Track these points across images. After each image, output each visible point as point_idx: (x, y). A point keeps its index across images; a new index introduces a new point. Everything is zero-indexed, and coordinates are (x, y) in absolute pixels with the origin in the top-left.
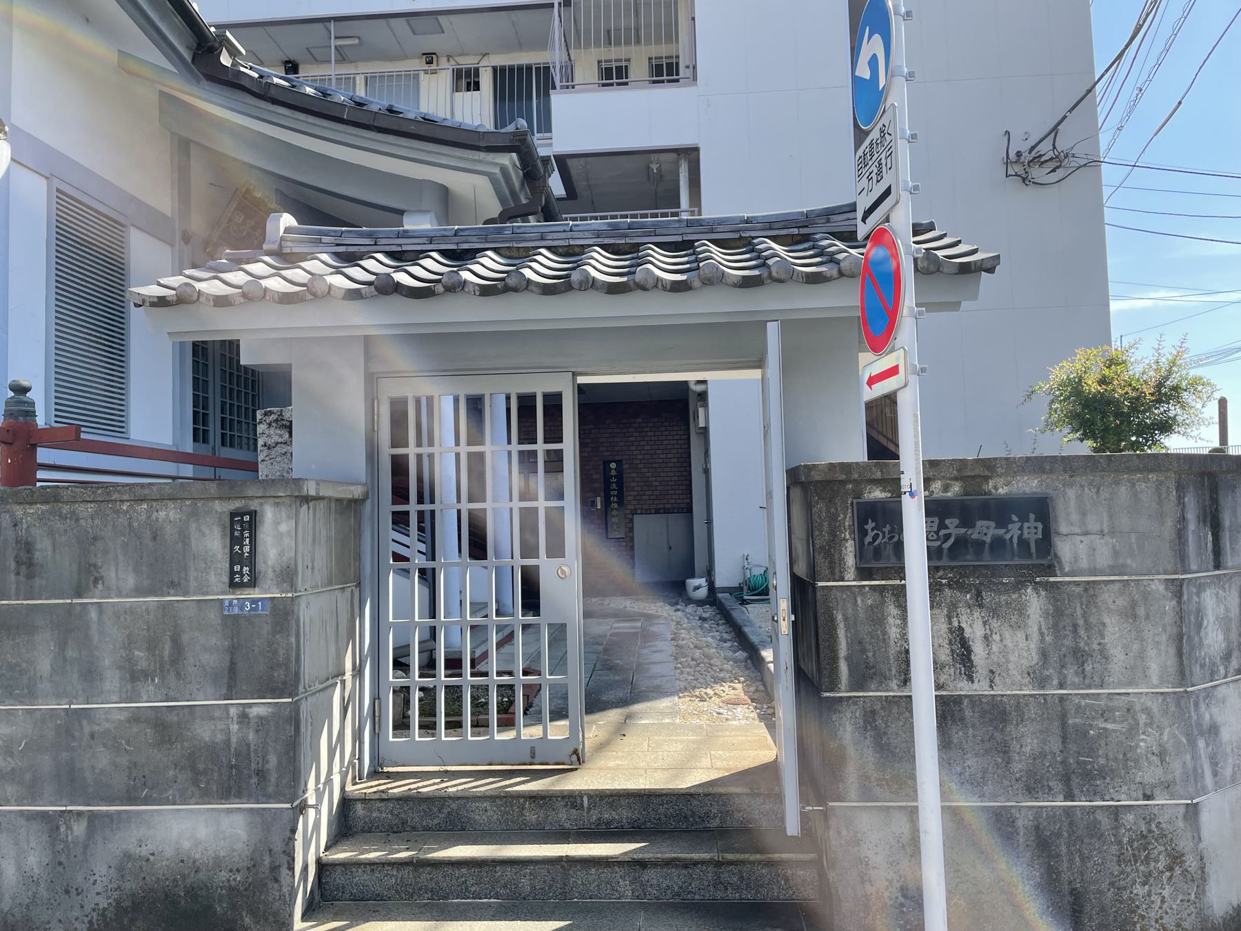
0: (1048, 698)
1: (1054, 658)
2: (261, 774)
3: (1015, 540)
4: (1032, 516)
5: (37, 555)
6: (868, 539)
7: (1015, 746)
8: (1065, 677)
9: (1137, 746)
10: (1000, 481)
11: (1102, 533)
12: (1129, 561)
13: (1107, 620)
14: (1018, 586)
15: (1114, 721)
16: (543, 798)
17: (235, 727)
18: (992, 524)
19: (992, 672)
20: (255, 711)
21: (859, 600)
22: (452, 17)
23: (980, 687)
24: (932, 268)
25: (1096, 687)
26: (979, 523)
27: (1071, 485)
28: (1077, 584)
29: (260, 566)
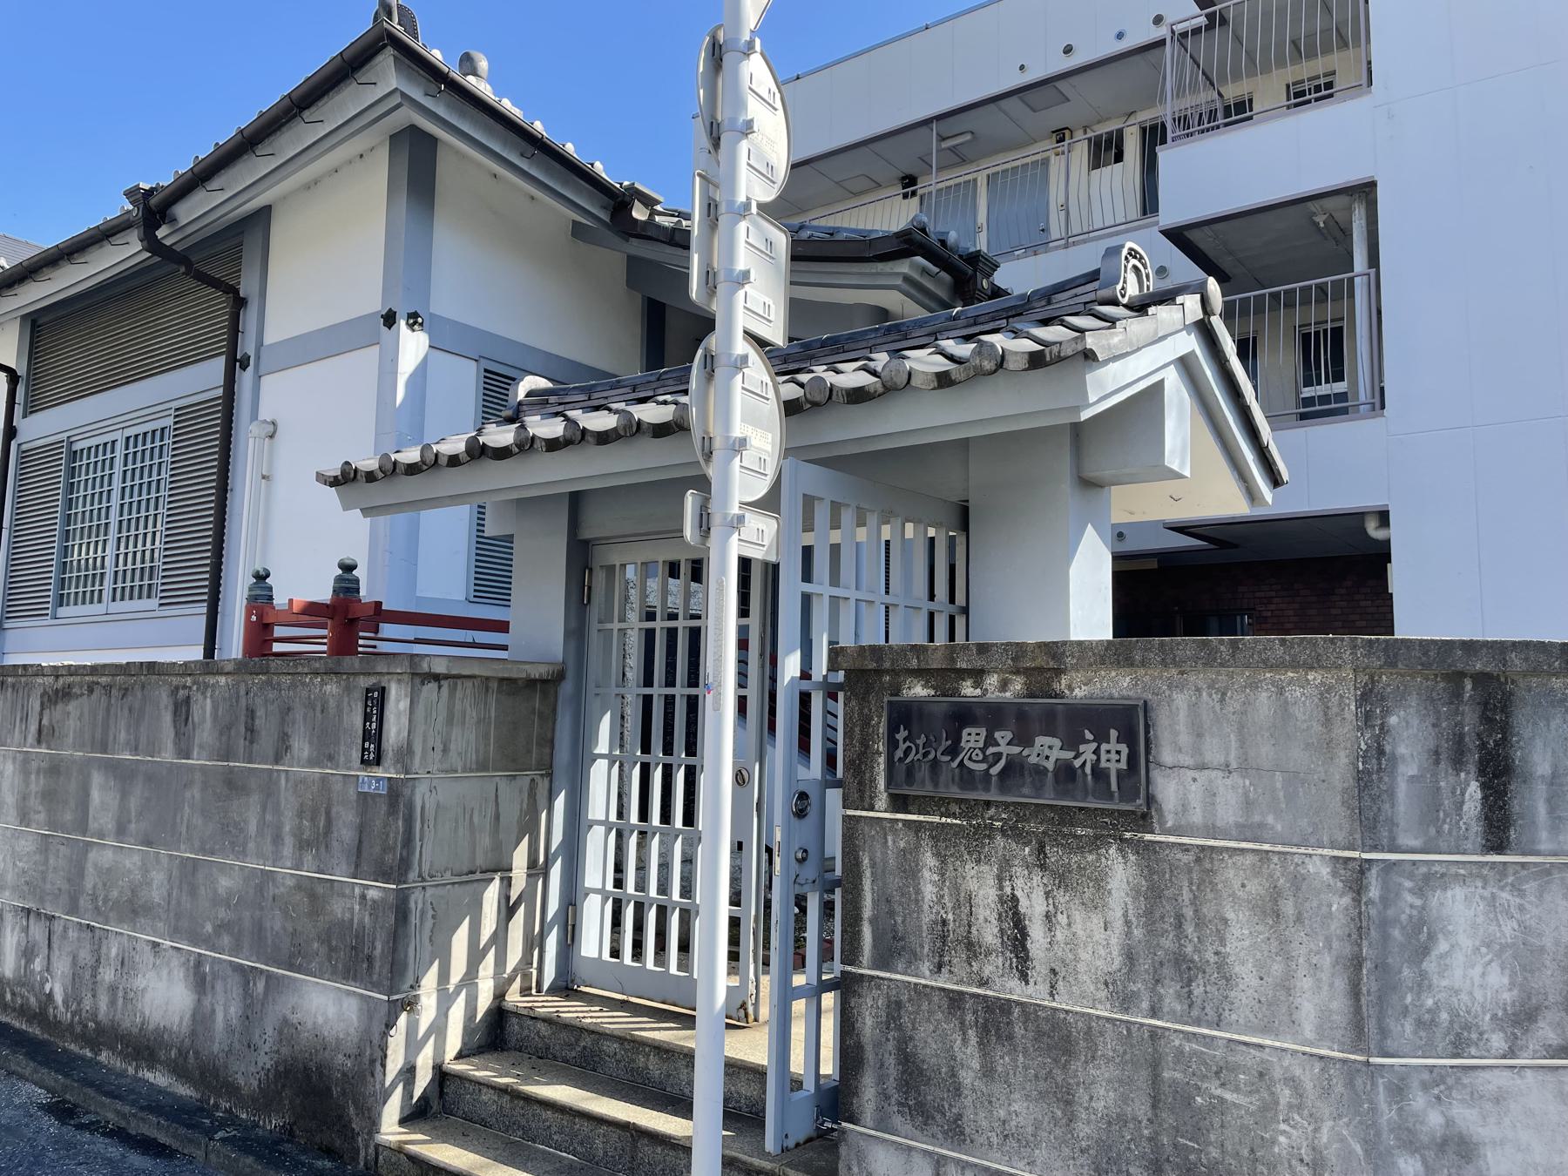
0: (1134, 1029)
1: (1144, 965)
2: (370, 959)
3: (1088, 770)
4: (1114, 734)
5: (257, 722)
6: (899, 754)
7: (1082, 1095)
8: (1161, 998)
9: (1274, 1142)
10: (1078, 677)
11: (1226, 768)
12: (1270, 819)
13: (1230, 915)
14: (1096, 843)
15: (1237, 1090)
16: (667, 1051)
17: (357, 907)
18: (1057, 742)
19: (1053, 971)
20: (372, 894)
21: (890, 838)
22: (1075, 80)
23: (1034, 992)
24: (988, 365)
25: (1209, 1026)
26: (1039, 740)
27: (1181, 687)
28: (1185, 848)
29: (384, 745)
